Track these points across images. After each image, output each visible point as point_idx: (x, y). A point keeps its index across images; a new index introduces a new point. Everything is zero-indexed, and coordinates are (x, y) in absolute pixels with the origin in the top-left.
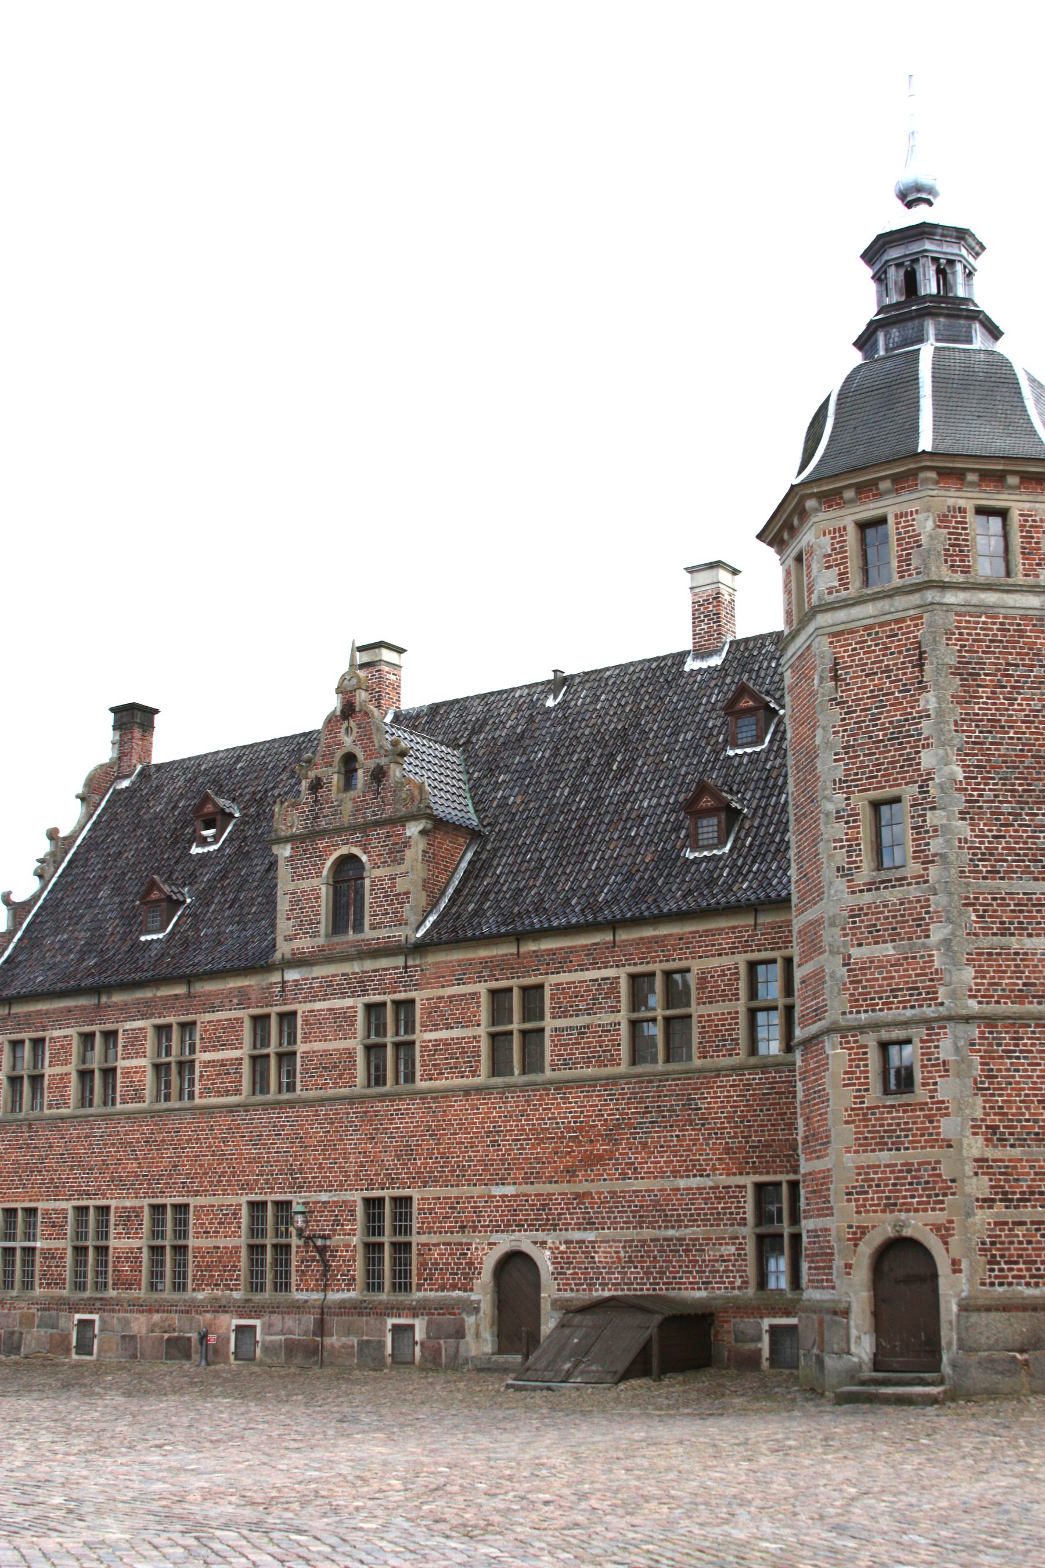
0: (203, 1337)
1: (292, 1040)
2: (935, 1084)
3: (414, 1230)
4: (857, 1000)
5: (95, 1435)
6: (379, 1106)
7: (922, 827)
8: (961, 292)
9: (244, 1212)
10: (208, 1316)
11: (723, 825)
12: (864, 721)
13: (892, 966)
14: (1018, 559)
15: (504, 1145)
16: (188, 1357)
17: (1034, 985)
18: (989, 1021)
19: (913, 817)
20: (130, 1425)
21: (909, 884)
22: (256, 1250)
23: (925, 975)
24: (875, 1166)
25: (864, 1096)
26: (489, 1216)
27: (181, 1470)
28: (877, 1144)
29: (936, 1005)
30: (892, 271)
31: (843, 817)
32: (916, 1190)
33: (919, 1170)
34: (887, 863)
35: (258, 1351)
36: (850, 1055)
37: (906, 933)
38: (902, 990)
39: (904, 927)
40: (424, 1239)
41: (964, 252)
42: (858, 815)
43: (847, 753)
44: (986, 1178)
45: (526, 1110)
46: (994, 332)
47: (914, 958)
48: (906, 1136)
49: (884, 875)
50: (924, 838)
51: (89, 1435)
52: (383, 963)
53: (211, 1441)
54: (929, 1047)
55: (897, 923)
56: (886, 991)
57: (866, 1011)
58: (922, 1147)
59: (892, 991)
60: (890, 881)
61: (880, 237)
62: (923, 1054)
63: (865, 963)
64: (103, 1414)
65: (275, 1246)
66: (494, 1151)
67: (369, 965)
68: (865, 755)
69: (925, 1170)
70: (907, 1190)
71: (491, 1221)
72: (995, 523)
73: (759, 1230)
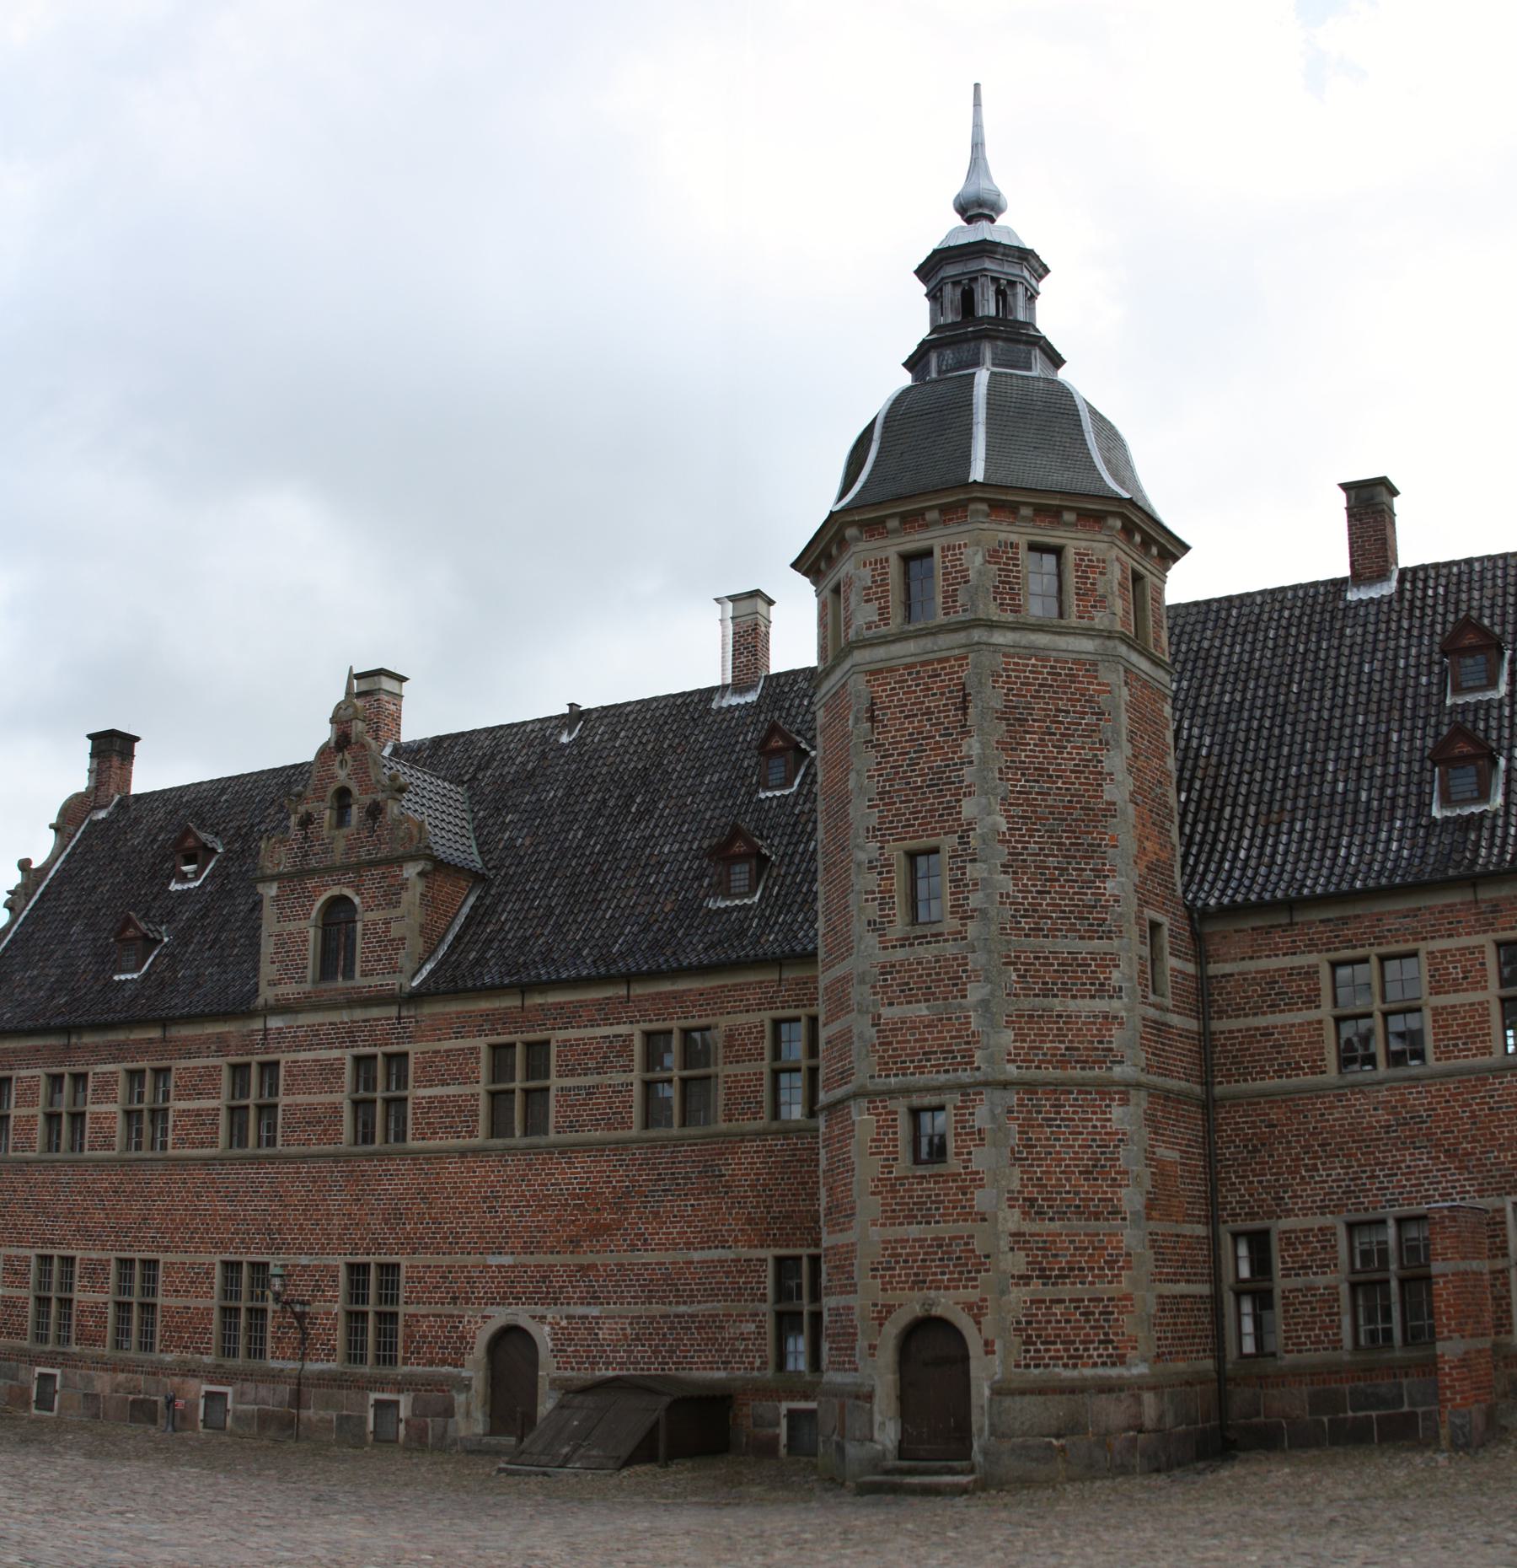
0: (170, 1402)
1: (274, 1091)
2: (970, 1153)
3: (401, 1300)
4: (887, 1063)
5: (54, 1495)
6: (365, 1166)
7: (962, 880)
8: (1021, 317)
9: (218, 1272)
10: (176, 1380)
11: (754, 873)
12: (902, 766)
14: (1072, 601)
16: (154, 1421)
17: (1077, 1049)
18: (1029, 1087)
19: (951, 869)
20: (92, 1488)
21: (946, 941)
22: (229, 1313)
24: (902, 1241)
25: (892, 1166)
27: (144, 1540)
28: (905, 1217)
29: (972, 1069)
30: (948, 289)
31: (876, 867)
32: (948, 1266)
33: (951, 1245)
34: (922, 917)
35: (229, 1420)
36: (878, 1121)
37: (940, 992)
38: (936, 1053)
39: (939, 987)
40: (411, 1309)
41: (1026, 274)
42: (892, 865)
43: (881, 799)
44: (1023, 1253)
46: (1057, 361)
47: (950, 1019)
48: (937, 1209)
49: (919, 930)
50: (963, 892)
51: (47, 1494)
52: (375, 1012)
53: (177, 1512)
54: (964, 1114)
55: (932, 981)
56: (918, 1054)
57: (896, 1075)
58: (955, 1221)
59: (924, 1054)
60: (925, 937)
61: (935, 252)
62: (956, 1122)
63: (896, 1023)
64: (62, 1474)
65: (250, 1310)
67: (359, 1014)
68: (901, 802)
69: (957, 1245)
70: (936, 1267)
72: (1049, 561)
73: (779, 1307)
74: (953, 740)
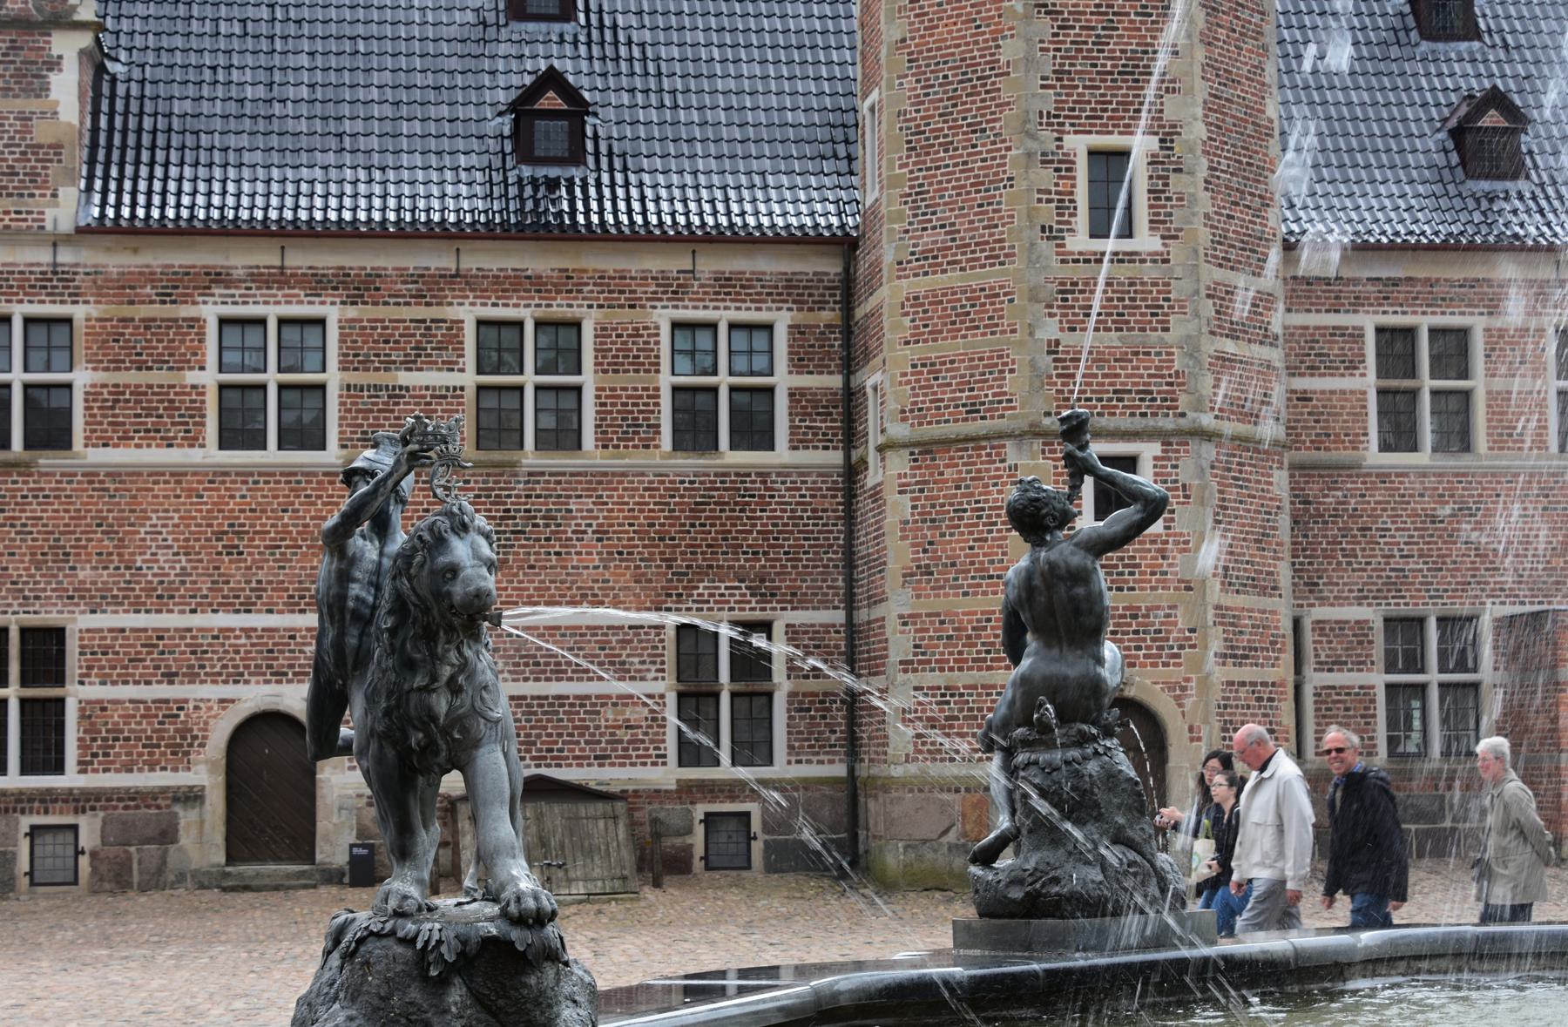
12: (1086, 43)
13: (1116, 360)
15: (250, 554)
23: (1162, 376)
26: (220, 659)
31: (1052, 162)
32: (1144, 640)
33: (1147, 616)
38: (1130, 392)
43: (1058, 79)
45: (293, 504)
47: (1148, 354)
48: (1132, 574)
54: (1165, 467)
55: (1125, 307)
56: (1107, 392)
58: (1152, 589)
59: (1115, 392)
66: (231, 562)
68: (1085, 87)
70: (1130, 640)
71: (225, 666)
74: (1153, 22)
